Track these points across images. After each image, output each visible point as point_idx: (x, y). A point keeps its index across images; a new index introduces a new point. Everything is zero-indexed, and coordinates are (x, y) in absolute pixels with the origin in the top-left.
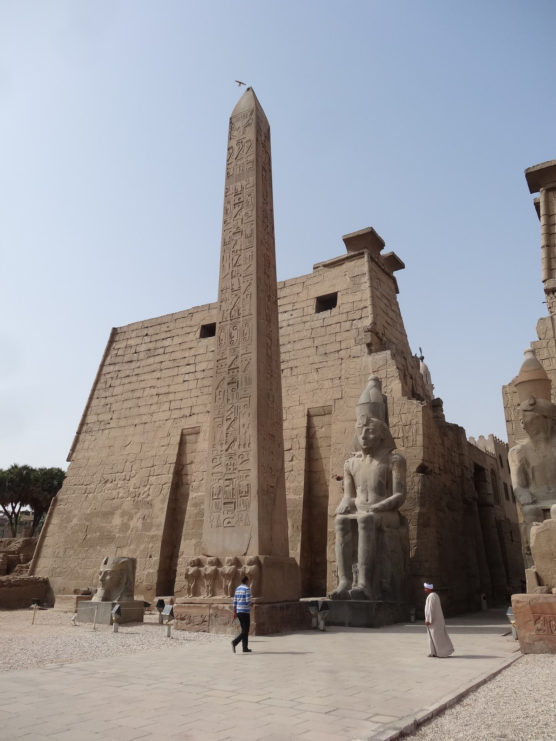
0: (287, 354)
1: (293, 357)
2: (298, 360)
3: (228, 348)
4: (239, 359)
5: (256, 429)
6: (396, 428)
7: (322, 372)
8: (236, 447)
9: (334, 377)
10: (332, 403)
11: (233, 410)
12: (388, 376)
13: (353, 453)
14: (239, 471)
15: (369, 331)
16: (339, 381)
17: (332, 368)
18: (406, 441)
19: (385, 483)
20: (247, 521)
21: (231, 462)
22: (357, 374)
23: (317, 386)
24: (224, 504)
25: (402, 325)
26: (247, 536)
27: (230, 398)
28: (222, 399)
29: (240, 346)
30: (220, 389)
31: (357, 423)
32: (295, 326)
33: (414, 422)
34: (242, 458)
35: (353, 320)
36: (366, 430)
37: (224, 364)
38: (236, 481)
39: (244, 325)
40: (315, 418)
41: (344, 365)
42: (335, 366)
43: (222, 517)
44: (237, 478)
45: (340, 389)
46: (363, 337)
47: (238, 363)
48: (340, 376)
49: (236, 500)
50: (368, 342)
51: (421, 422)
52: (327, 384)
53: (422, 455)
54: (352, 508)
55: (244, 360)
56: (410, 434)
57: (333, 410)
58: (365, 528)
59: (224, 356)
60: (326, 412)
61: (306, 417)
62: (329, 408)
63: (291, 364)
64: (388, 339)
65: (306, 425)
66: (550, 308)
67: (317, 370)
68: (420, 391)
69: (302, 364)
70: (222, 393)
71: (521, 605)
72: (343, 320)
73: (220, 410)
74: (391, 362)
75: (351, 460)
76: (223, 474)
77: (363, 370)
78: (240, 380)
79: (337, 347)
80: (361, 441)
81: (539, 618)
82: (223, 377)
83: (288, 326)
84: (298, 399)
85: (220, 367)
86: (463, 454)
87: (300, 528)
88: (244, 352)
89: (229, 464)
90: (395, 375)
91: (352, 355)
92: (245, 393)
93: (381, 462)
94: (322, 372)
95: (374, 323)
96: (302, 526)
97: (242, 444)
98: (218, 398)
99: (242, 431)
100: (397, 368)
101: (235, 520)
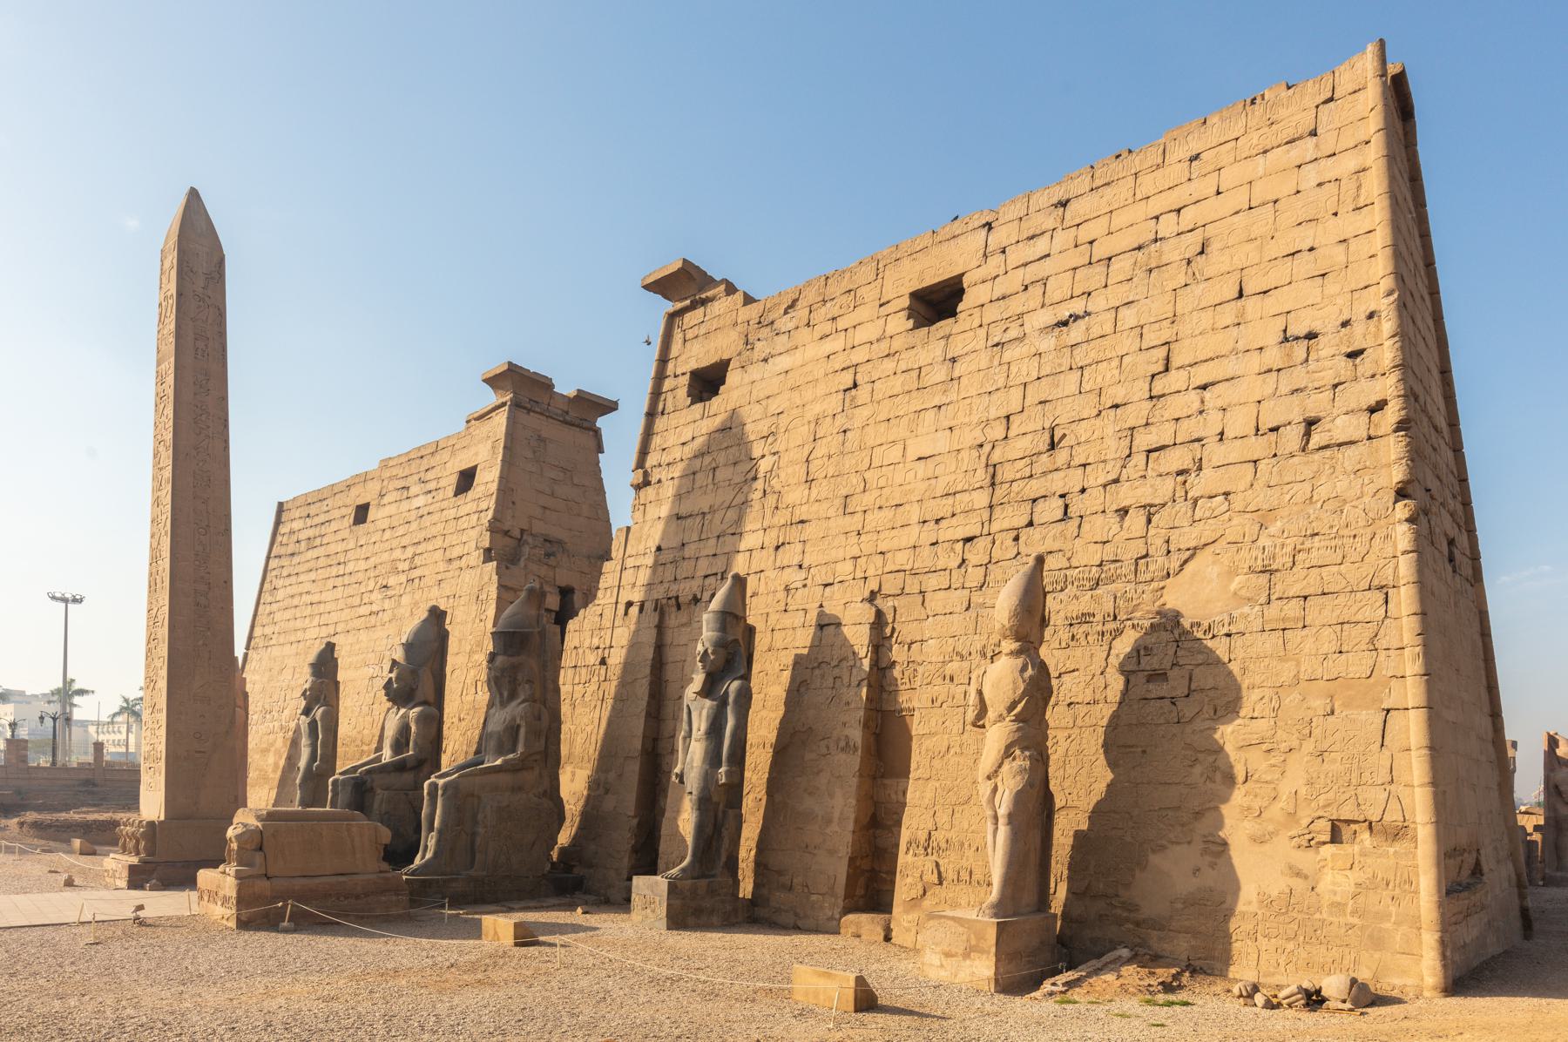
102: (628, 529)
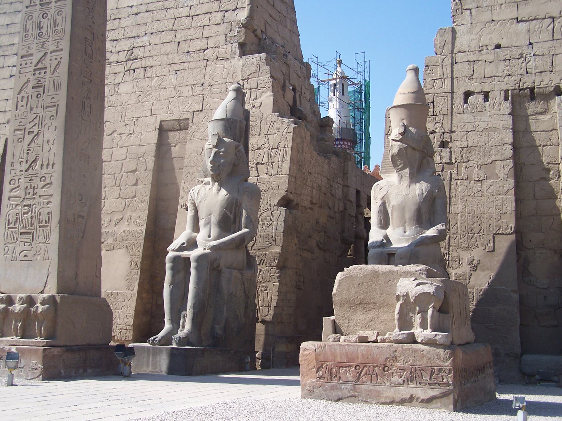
0: (142, 49)
1: (148, 54)
2: (155, 58)
3: (36, 41)
4: (48, 57)
5: (62, 147)
6: (261, 151)
7: (181, 76)
8: (38, 167)
9: (195, 82)
10: (189, 116)
11: (36, 121)
12: (259, 86)
13: (201, 179)
14: (40, 196)
15: (243, 27)
16: (202, 88)
17: (195, 71)
18: (270, 167)
19: (232, 216)
20: (46, 255)
21: (31, 185)
22: (223, 81)
23: (174, 93)
24: (21, 234)
25: (294, 22)
26: (45, 272)
27: (34, 106)
28: (25, 107)
29: (50, 39)
30: (23, 93)
31: (207, 143)
32: (155, 13)
33: (282, 145)
34: (44, 181)
35: (226, 11)
36: (215, 153)
37: (29, 62)
38: (35, 208)
39: (56, 13)
40: (171, 134)
41: (208, 68)
42: (199, 69)
43: (18, 249)
44: (37, 204)
45: (201, 99)
46: (236, 34)
47: (46, 62)
48: (202, 82)
49: (35, 230)
50: (241, 41)
51: (290, 145)
52: (187, 91)
53: (287, 185)
54: (192, 244)
55: (53, 58)
56: (276, 160)
57: (190, 125)
58: (197, 268)
59: (60, 47)
60: (182, 125)
62: (186, 122)
63: (144, 63)
64: (270, 38)
65: (156, 141)
66: (453, 16)
68: (305, 108)
69: (159, 64)
70: (25, 99)
71: (307, 352)
72: (213, 10)
73: (22, 120)
74: (266, 68)
75: (197, 188)
76: (22, 199)
77: (231, 77)
78: (46, 83)
79: (202, 44)
80: (209, 166)
81: (322, 365)
82: (27, 78)
83: (147, 12)
85: (24, 65)
86: (348, 186)
87: (139, 264)
88: (54, 48)
89: (29, 188)
90: (268, 86)
91: (221, 56)
92: (53, 100)
93: (229, 192)
94: (181, 76)
95: (250, 17)
96: (142, 263)
97: (45, 164)
98: (20, 104)
99: (46, 147)
100: (272, 76)
101: (33, 252)
102: (453, 31)
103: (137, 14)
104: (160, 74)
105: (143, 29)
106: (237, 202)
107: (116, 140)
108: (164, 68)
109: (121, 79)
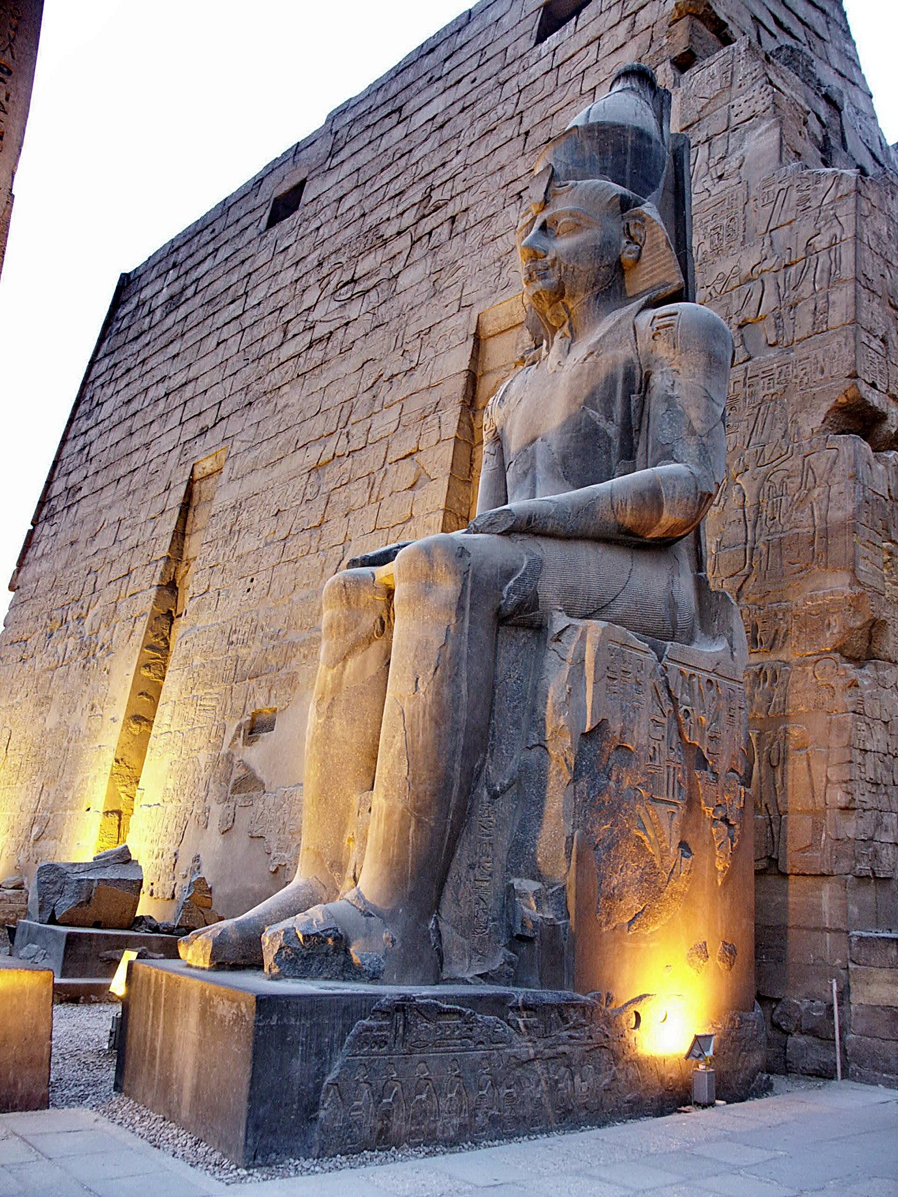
0: (449, 185)
19: (612, 430)
33: (821, 242)
61: (471, 343)
67: (519, 195)
84: (459, 296)
103: (442, 127)
104: (485, 215)
105: (454, 146)
106: (629, 377)
107: (381, 395)
108: (493, 200)
109: (403, 263)
